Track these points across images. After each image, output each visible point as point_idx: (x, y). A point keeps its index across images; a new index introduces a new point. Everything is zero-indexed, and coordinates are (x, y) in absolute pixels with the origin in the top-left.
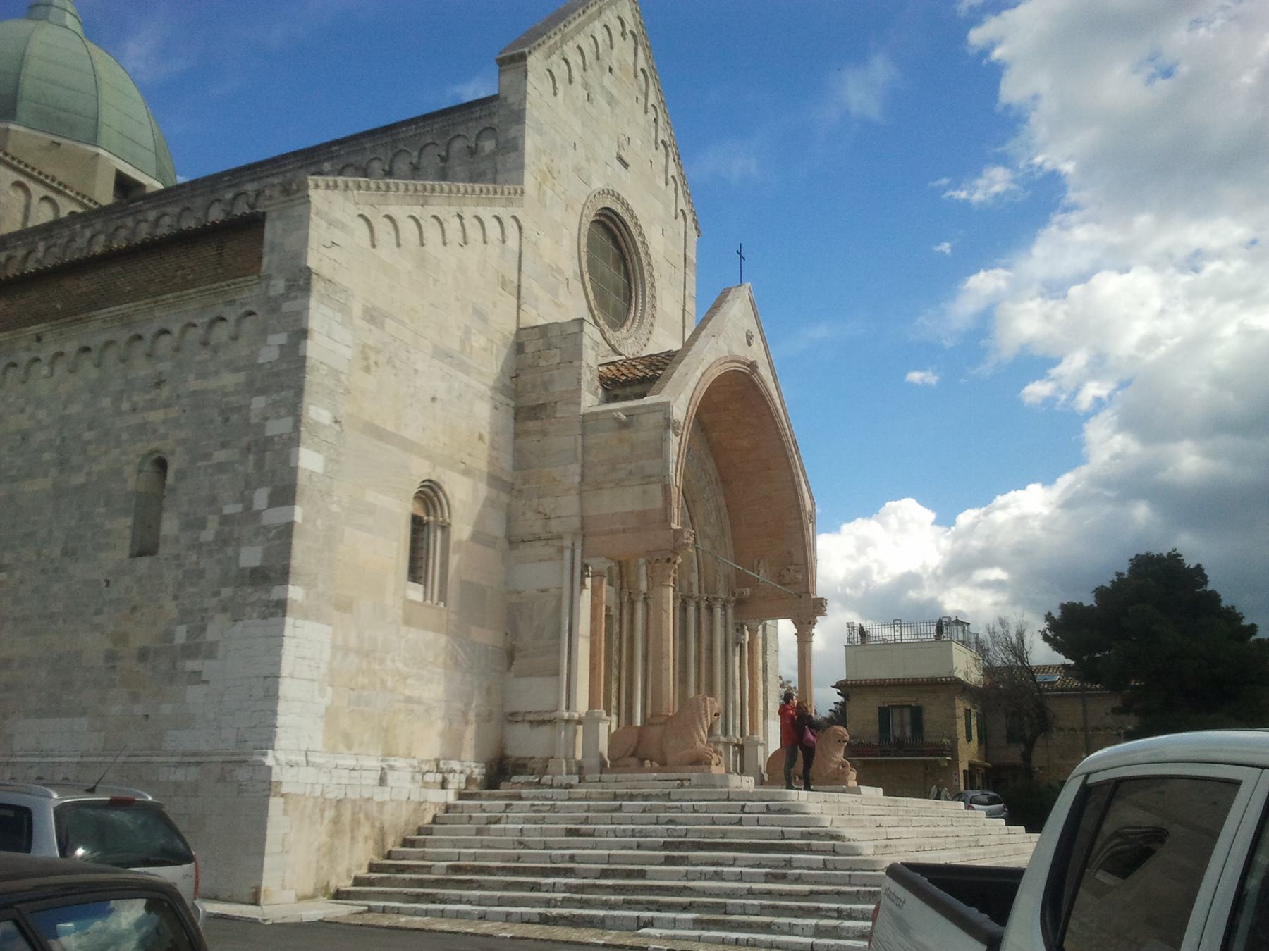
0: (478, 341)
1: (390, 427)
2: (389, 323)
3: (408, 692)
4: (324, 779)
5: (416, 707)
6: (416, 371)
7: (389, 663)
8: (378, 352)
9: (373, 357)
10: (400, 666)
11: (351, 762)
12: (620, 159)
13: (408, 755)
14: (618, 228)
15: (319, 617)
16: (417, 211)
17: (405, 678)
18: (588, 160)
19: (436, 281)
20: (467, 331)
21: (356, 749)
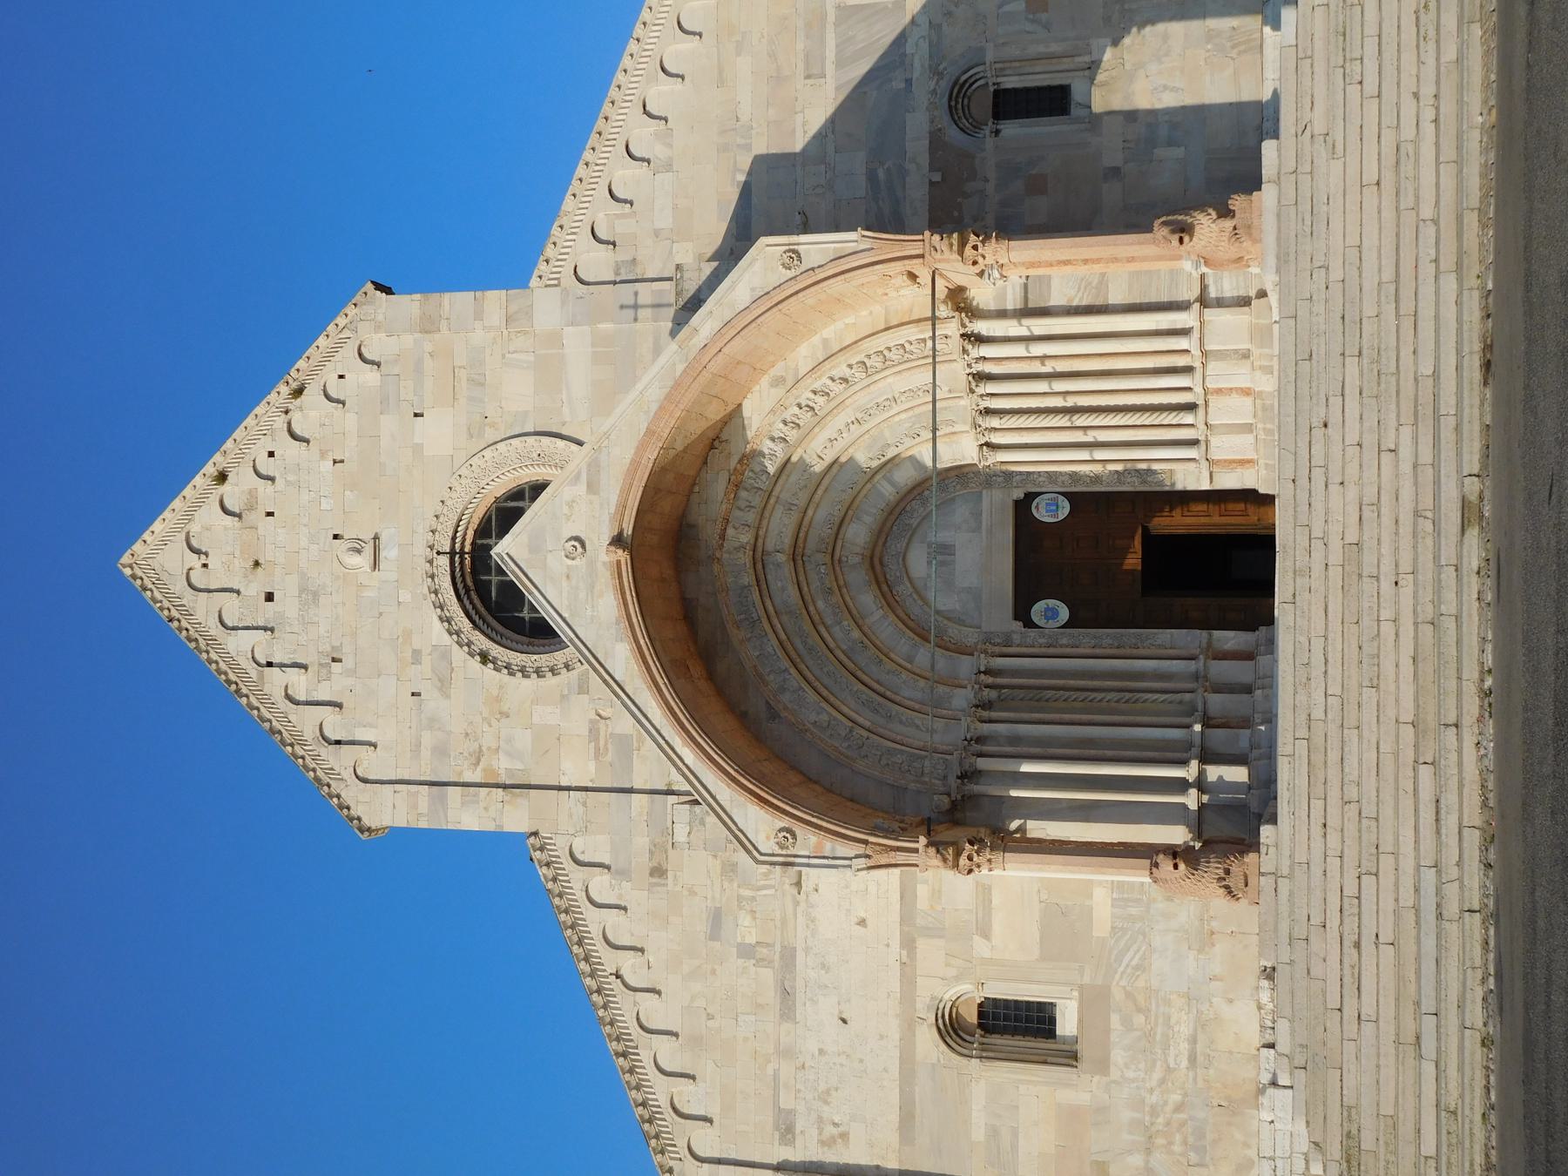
0: (747, 930)
1: (894, 1098)
2: (786, 1102)
3: (1185, 1063)
5: (1199, 1047)
6: (821, 1051)
7: (1154, 1099)
8: (820, 1120)
9: (830, 1130)
10: (1157, 1075)
12: (375, 565)
13: (1256, 1058)
14: (464, 539)
16: (645, 1057)
17: (1169, 1070)
18: (417, 656)
19: (710, 1017)
20: (746, 951)
21: (1252, 1153)
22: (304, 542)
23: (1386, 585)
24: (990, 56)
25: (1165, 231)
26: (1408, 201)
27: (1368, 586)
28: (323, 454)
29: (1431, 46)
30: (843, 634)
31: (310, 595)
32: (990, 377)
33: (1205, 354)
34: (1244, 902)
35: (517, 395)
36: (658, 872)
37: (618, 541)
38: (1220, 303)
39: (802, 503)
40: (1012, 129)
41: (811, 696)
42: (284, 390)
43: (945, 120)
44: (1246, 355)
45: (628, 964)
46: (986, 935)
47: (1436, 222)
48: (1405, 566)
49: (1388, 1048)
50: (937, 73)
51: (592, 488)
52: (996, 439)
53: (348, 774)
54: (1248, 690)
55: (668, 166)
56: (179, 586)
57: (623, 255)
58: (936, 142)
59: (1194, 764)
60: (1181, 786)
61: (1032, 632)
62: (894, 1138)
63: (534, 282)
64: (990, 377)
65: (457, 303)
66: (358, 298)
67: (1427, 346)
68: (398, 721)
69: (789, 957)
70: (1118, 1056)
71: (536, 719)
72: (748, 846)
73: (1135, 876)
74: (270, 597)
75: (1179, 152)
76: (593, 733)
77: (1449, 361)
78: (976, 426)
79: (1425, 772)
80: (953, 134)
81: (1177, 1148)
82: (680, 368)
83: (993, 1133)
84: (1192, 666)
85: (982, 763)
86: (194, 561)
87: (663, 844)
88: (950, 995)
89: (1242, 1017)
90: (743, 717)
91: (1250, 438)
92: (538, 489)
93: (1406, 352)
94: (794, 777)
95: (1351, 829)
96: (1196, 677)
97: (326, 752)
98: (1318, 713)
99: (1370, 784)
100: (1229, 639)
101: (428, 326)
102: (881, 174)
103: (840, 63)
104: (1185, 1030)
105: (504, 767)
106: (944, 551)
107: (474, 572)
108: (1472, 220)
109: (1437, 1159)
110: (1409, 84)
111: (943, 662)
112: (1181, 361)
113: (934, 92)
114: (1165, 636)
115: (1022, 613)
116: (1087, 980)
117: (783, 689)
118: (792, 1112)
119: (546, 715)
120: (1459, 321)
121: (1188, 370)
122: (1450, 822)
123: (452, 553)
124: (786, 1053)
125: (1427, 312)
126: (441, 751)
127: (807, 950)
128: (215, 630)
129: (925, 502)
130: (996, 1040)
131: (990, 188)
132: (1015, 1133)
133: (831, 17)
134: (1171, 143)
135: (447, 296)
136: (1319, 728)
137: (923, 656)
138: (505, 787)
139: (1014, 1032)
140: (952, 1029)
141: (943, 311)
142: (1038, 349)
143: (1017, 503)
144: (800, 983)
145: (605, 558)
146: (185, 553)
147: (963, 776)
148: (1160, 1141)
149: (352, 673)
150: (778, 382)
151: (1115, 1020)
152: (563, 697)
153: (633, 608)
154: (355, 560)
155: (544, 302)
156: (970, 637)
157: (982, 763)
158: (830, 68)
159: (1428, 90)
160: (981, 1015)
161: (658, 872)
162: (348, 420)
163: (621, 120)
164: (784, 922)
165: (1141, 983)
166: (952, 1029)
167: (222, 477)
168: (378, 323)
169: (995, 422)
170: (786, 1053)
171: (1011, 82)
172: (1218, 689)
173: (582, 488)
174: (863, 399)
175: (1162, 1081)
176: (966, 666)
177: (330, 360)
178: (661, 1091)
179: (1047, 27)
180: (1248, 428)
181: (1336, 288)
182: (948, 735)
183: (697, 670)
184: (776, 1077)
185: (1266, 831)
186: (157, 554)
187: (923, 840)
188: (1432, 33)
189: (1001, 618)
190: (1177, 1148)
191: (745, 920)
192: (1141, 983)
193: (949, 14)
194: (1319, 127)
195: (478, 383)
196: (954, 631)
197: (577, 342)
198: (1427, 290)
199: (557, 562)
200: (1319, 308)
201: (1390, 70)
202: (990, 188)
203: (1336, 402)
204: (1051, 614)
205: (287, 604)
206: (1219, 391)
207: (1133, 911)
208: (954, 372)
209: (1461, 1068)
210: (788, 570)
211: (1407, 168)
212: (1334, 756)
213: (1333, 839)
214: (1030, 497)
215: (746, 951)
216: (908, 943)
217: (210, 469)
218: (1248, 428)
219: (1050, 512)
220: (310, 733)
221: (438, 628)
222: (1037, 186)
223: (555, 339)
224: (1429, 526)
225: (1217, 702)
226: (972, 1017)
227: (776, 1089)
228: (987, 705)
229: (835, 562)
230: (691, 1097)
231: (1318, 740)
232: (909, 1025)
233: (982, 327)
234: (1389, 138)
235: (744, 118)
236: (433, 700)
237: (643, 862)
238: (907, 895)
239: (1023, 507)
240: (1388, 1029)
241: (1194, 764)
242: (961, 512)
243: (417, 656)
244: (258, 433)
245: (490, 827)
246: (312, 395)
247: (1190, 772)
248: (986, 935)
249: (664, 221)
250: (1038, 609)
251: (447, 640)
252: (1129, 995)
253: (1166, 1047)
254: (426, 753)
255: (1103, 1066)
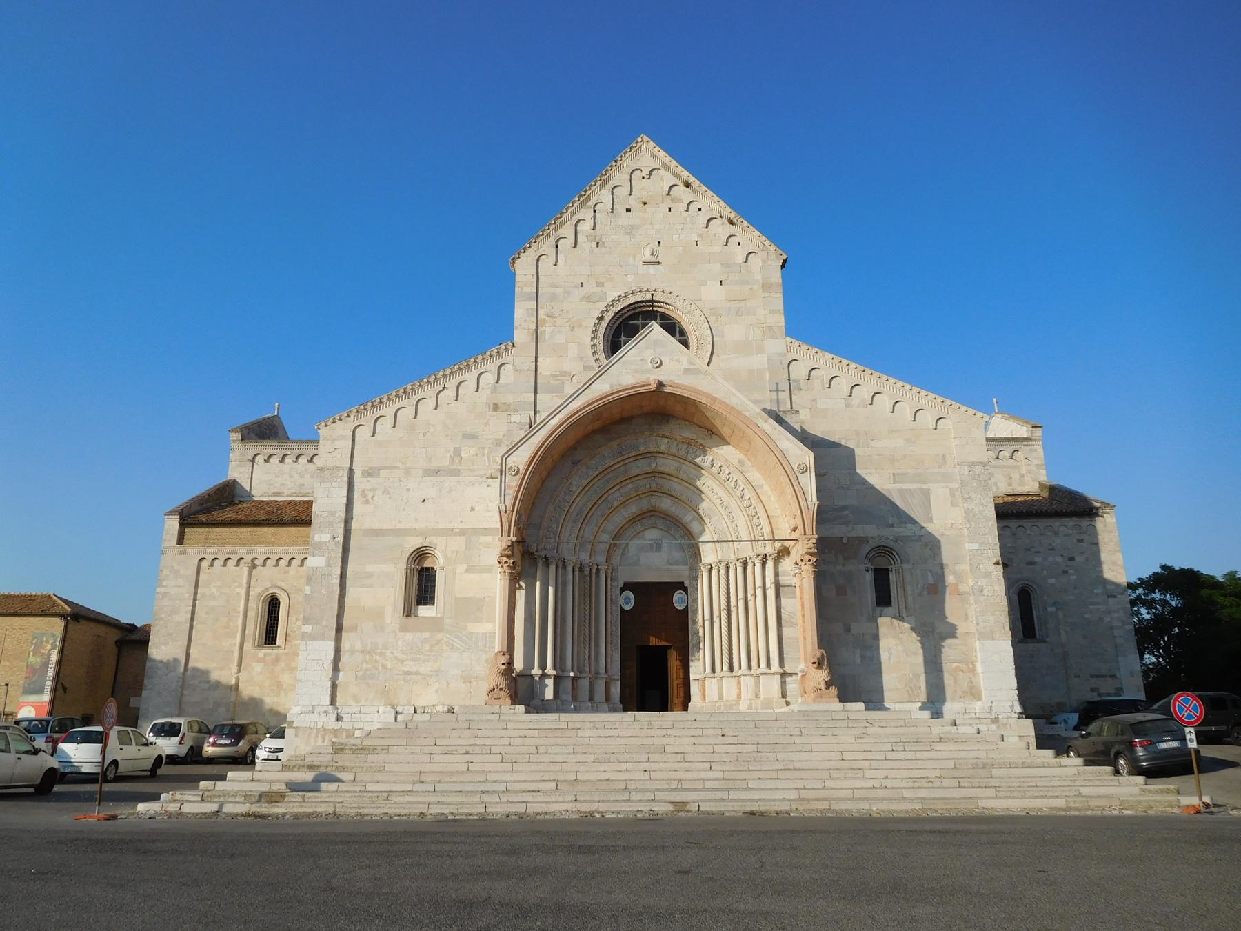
0: (468, 452)
4: (324, 718)
7: (388, 654)
8: (375, 490)
9: (370, 494)
10: (401, 656)
11: (356, 709)
15: (323, 637)
16: (404, 403)
17: (402, 662)
18: (601, 284)
19: (424, 434)
20: (457, 452)
21: (363, 703)
22: (657, 227)
23: (644, 766)
24: (905, 566)
25: (819, 655)
26: (834, 774)
27: (644, 757)
28: (700, 235)
29: (911, 785)
30: (616, 497)
31: (630, 231)
32: (745, 569)
33: (758, 676)
34: (486, 698)
35: (732, 332)
36: (496, 407)
37: (660, 384)
38: (783, 683)
39: (681, 476)
40: (869, 577)
41: (585, 482)
42: (732, 215)
43: (873, 544)
44: (757, 696)
45: (450, 393)
46: (467, 571)
47: (824, 788)
48: (654, 775)
49: (418, 768)
50: (897, 539)
51: (687, 371)
52: (714, 572)
53: (541, 252)
54: (591, 699)
55: (848, 406)
56: (633, 165)
57: (803, 383)
58: (863, 540)
59: (554, 673)
60: (543, 666)
61: (618, 592)
62: (366, 526)
63: (789, 339)
64: (745, 569)
65: (778, 301)
66: (779, 251)
67: (762, 785)
68: (567, 277)
69: (455, 473)
70: (409, 636)
71: (571, 345)
72: (510, 452)
73: (498, 644)
74: (628, 210)
75: (858, 660)
76: (564, 374)
77: (755, 795)
78: (721, 562)
79: (553, 785)
80: (867, 549)
81: (364, 666)
82: (747, 414)
83: (370, 575)
84: (602, 671)
85: (552, 568)
86: (646, 172)
87: (510, 410)
88: (438, 553)
89: (429, 697)
90: (574, 448)
91: (716, 699)
92: (685, 343)
93: (760, 774)
94: (545, 473)
95: (524, 749)
96: (597, 673)
97: (552, 241)
98: (580, 733)
99: (546, 759)
100: (616, 690)
101: (766, 287)
102: (846, 513)
103: (901, 491)
104: (422, 669)
105: (546, 329)
106: (658, 547)
107: (643, 312)
108: (825, 805)
109: (365, 791)
110: (892, 774)
111: (603, 548)
112: (754, 664)
113: (887, 538)
114: (617, 657)
115: (627, 586)
116: (447, 621)
117: (588, 468)
118: (378, 475)
119: (573, 350)
120: (775, 800)
121: (750, 667)
122: (528, 797)
123: (652, 301)
124: (407, 472)
125: (779, 784)
126: (553, 298)
127: (458, 482)
128: (611, 184)
129: (682, 537)
130: (416, 577)
131: (839, 567)
132: (371, 586)
133: (924, 486)
134: (863, 657)
135: (781, 296)
136: (573, 733)
137: (605, 537)
138: (536, 330)
139: (420, 585)
140: (420, 555)
141: (778, 545)
142: (759, 593)
143: (682, 583)
144: (442, 478)
145: (651, 378)
146: (650, 167)
147: (546, 558)
148: (368, 658)
149: (592, 252)
150: (741, 462)
151: (427, 635)
152: (582, 358)
153: (627, 393)
154: (648, 253)
155: (779, 345)
156: (615, 561)
157: (552, 568)
158: (898, 486)
159: (889, 783)
160: (428, 569)
161: (496, 407)
162: (718, 248)
163: (871, 382)
164: (473, 470)
165: (445, 647)
166: (420, 555)
167: (688, 185)
168: (766, 262)
169: (723, 571)
170: (407, 472)
171: (892, 576)
172: (591, 684)
173: (686, 366)
174: (733, 505)
175: (397, 658)
176: (601, 559)
177: (748, 238)
178: (388, 411)
179: (920, 594)
180: (721, 697)
181: (790, 740)
182: (566, 551)
183: (597, 425)
184: (395, 467)
185: (522, 708)
186: (648, 154)
187: (514, 539)
188: (917, 785)
189: (625, 576)
190: (364, 666)
191: (472, 451)
192: (445, 647)
193: (926, 545)
194: (871, 730)
195: (738, 312)
196: (618, 552)
197: (758, 362)
198: (791, 784)
199: (649, 354)
200: (781, 731)
201: (898, 764)
202: (839, 567)
203: (734, 740)
204: (627, 602)
205: (625, 219)
206: (739, 683)
207: (481, 644)
208: (747, 551)
209: (409, 802)
210: (647, 469)
211: (850, 774)
212: (559, 741)
213: (519, 741)
214: (686, 590)
215: (457, 452)
216: (463, 532)
217: (692, 179)
218: (721, 697)
219: (678, 599)
220: (561, 232)
221: (615, 295)
222: (841, 591)
223: (760, 351)
224: (673, 786)
225: (584, 684)
226: (427, 564)
227: (390, 468)
228: (581, 569)
229: (651, 493)
230: (385, 425)
231: (568, 733)
232: (423, 533)
233: (770, 564)
234: (866, 764)
235: (873, 443)
236: (578, 293)
237: (501, 399)
238: (486, 531)
239: (681, 586)
240: (428, 768)
241: (554, 673)
242: (678, 555)
243: (602, 284)
244: (710, 202)
245: (516, 323)
246: (730, 229)
247: (550, 670)
248: (467, 571)
249: (821, 404)
250: (631, 595)
251: (609, 300)
252: (438, 642)
253: (414, 660)
254: (552, 290)
255: (404, 629)
